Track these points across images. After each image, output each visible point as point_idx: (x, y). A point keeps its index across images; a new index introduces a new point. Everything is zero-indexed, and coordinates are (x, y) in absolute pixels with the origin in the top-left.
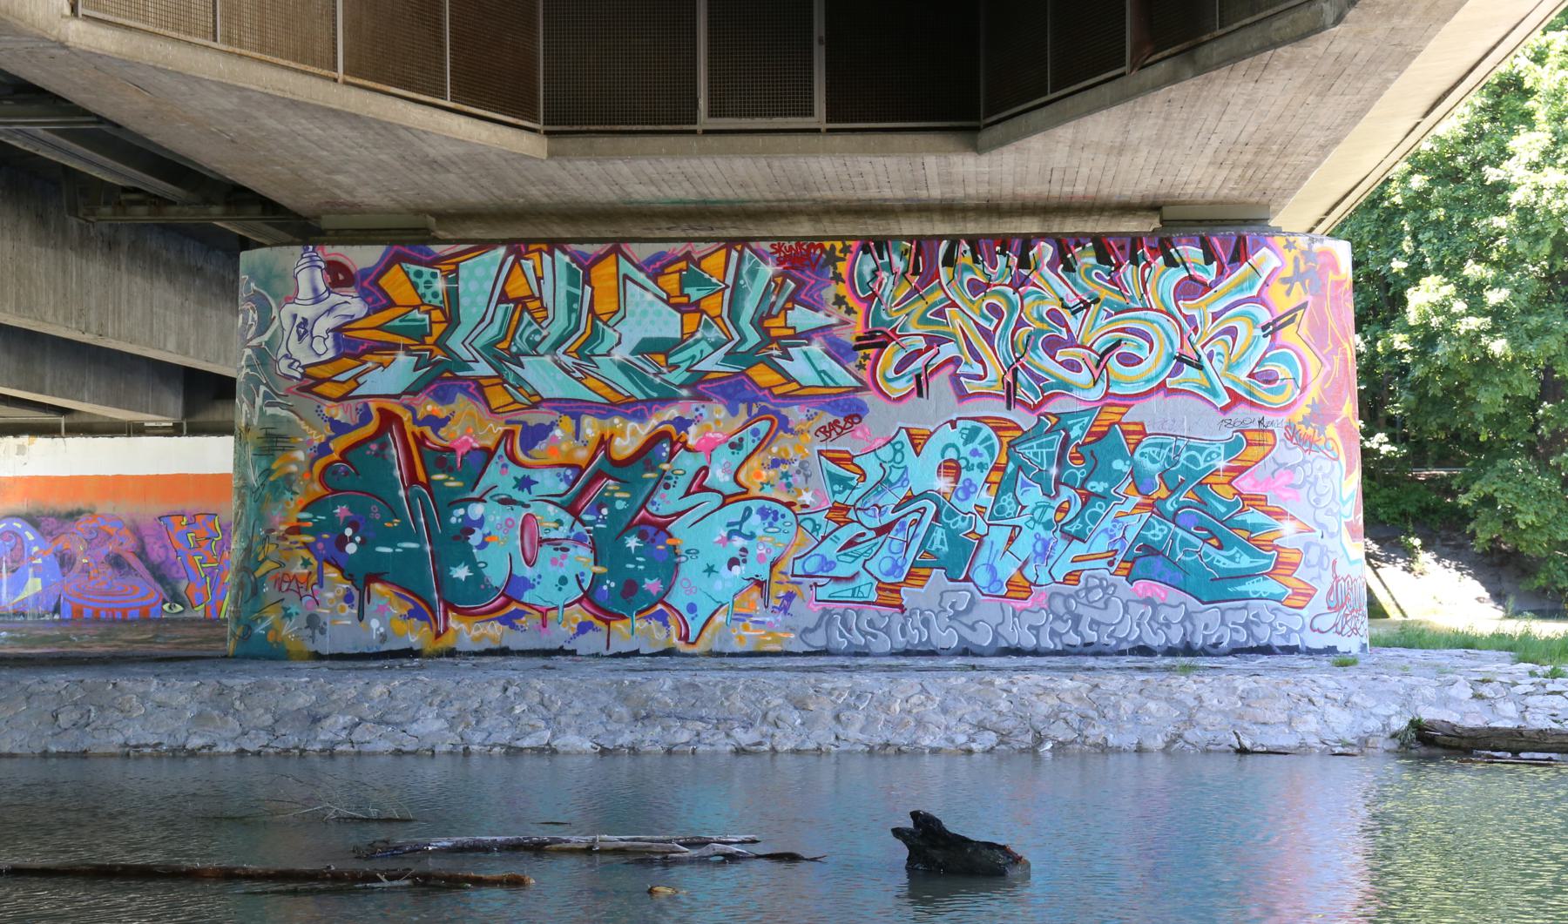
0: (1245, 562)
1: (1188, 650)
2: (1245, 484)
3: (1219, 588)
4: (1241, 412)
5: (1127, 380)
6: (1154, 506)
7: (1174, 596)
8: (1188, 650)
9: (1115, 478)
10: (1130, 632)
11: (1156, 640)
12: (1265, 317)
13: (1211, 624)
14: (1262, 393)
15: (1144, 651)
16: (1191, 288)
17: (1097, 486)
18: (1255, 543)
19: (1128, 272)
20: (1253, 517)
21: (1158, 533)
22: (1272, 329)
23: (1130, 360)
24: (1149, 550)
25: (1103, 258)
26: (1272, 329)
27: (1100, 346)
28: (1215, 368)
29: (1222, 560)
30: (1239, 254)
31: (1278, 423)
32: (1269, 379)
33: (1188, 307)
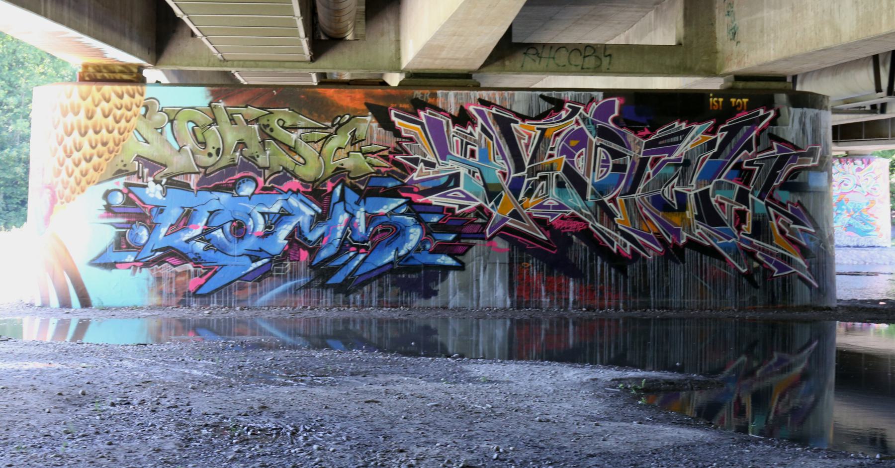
0: (870, 228)
1: (858, 246)
2: (870, 211)
3: (865, 233)
4: (869, 197)
5: (845, 189)
6: (851, 216)
7: (855, 235)
8: (858, 246)
9: (843, 210)
10: (846, 243)
11: (851, 244)
12: (874, 176)
13: (863, 241)
14: (874, 192)
15: (848, 246)
16: (859, 170)
17: (839, 211)
18: (872, 225)
19: (846, 166)
20: (871, 218)
21: (851, 222)
22: (876, 178)
23: (846, 185)
24: (850, 225)
25: (840, 162)
26: (876, 178)
27: (840, 181)
28: (864, 187)
29: (865, 228)
30: (869, 163)
31: (876, 199)
32: (875, 189)
33: (858, 174)
